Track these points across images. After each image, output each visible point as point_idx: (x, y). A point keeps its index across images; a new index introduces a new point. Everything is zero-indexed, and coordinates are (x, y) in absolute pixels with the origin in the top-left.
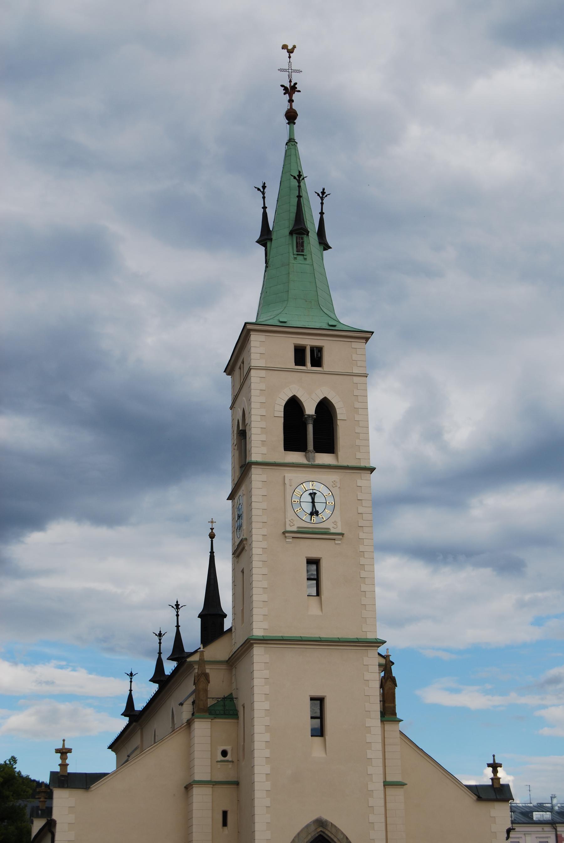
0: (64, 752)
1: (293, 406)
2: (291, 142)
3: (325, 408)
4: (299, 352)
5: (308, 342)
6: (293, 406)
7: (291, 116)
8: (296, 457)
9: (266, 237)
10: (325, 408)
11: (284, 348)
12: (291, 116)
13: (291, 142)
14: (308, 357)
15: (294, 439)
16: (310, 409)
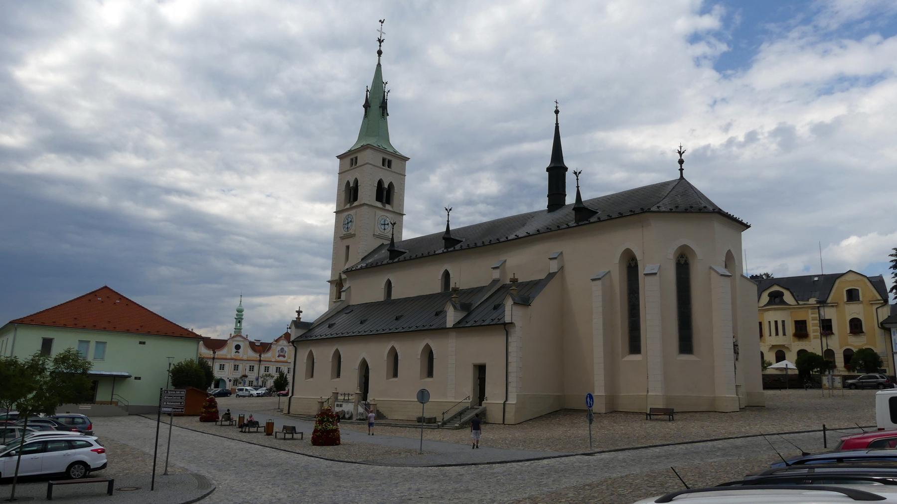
0: (299, 312)
1: (380, 183)
2: (379, 65)
3: (391, 185)
4: (384, 160)
5: (388, 157)
6: (380, 183)
7: (380, 53)
8: (379, 204)
9: (367, 106)
10: (391, 185)
11: (378, 159)
12: (380, 53)
13: (379, 65)
14: (387, 163)
15: (379, 198)
16: (386, 186)
